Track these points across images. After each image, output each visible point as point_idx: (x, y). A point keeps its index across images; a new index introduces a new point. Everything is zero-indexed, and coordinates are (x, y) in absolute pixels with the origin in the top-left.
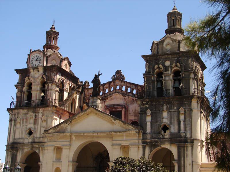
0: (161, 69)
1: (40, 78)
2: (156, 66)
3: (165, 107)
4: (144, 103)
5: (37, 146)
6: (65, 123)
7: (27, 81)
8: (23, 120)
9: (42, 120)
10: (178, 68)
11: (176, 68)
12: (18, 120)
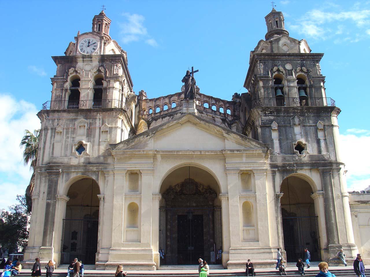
0: (281, 73)
1: (95, 70)
2: (275, 69)
3: (297, 120)
4: (267, 112)
5: (95, 169)
6: (145, 135)
7: (71, 74)
8: (67, 129)
9: (101, 131)
10: (303, 73)
11: (300, 73)
12: (59, 129)
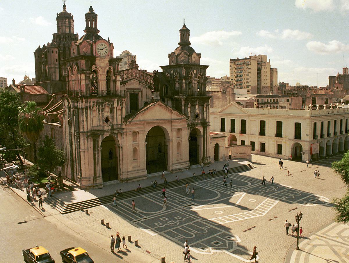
5: (117, 132)
